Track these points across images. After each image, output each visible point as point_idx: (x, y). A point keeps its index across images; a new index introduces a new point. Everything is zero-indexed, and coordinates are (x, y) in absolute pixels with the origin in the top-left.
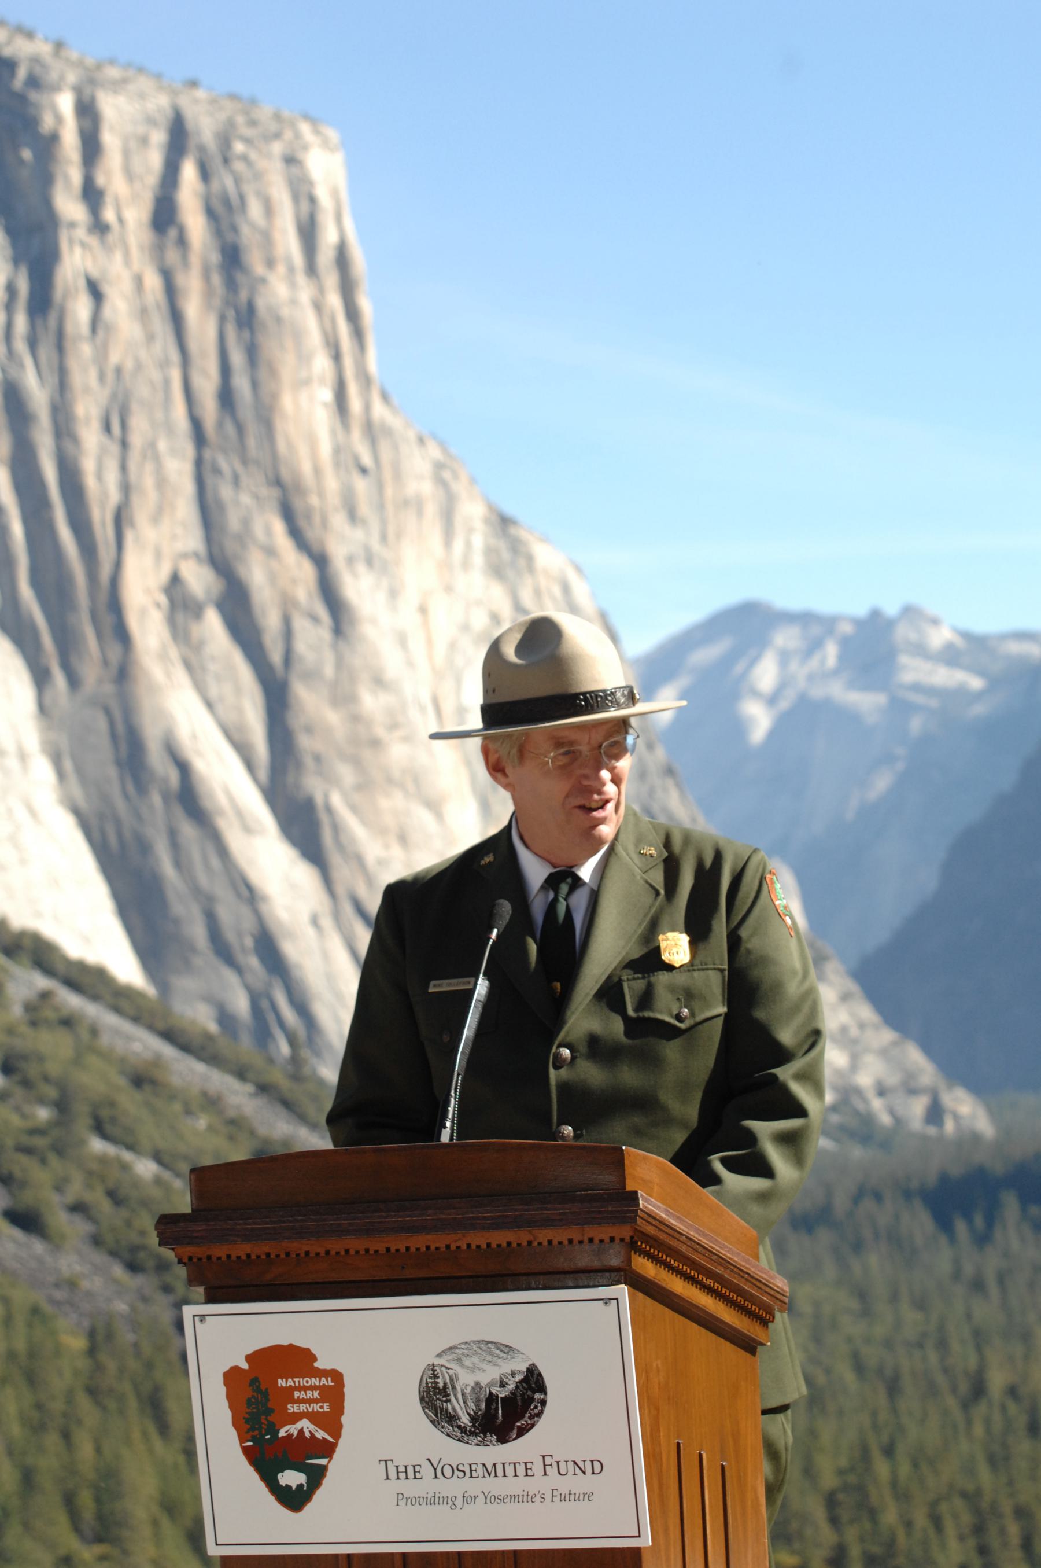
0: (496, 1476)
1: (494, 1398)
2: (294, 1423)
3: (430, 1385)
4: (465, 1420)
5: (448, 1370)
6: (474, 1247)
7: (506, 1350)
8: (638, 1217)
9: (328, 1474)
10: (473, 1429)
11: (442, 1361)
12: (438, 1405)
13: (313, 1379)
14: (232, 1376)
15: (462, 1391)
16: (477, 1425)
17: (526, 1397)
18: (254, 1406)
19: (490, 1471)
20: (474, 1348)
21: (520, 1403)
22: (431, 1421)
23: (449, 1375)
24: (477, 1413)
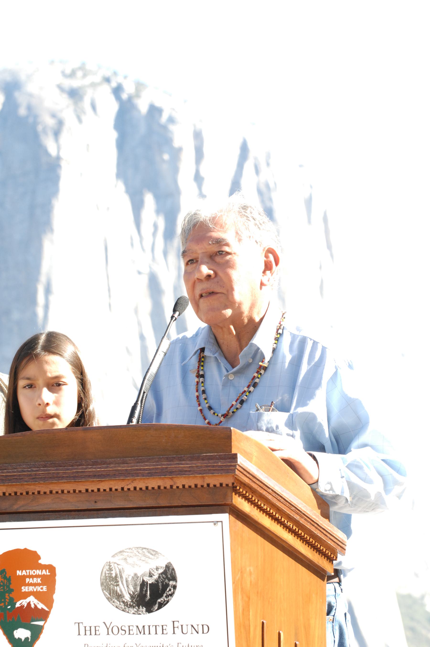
0: (144, 634)
2: (25, 599)
3: (107, 575)
4: (127, 598)
5: (118, 566)
7: (153, 553)
8: (236, 470)
9: (44, 631)
10: (132, 604)
11: (115, 560)
12: (111, 588)
13: (38, 571)
15: (126, 579)
17: (165, 583)
19: (141, 631)
21: (161, 587)
22: (107, 598)
23: (119, 569)
24: (135, 593)
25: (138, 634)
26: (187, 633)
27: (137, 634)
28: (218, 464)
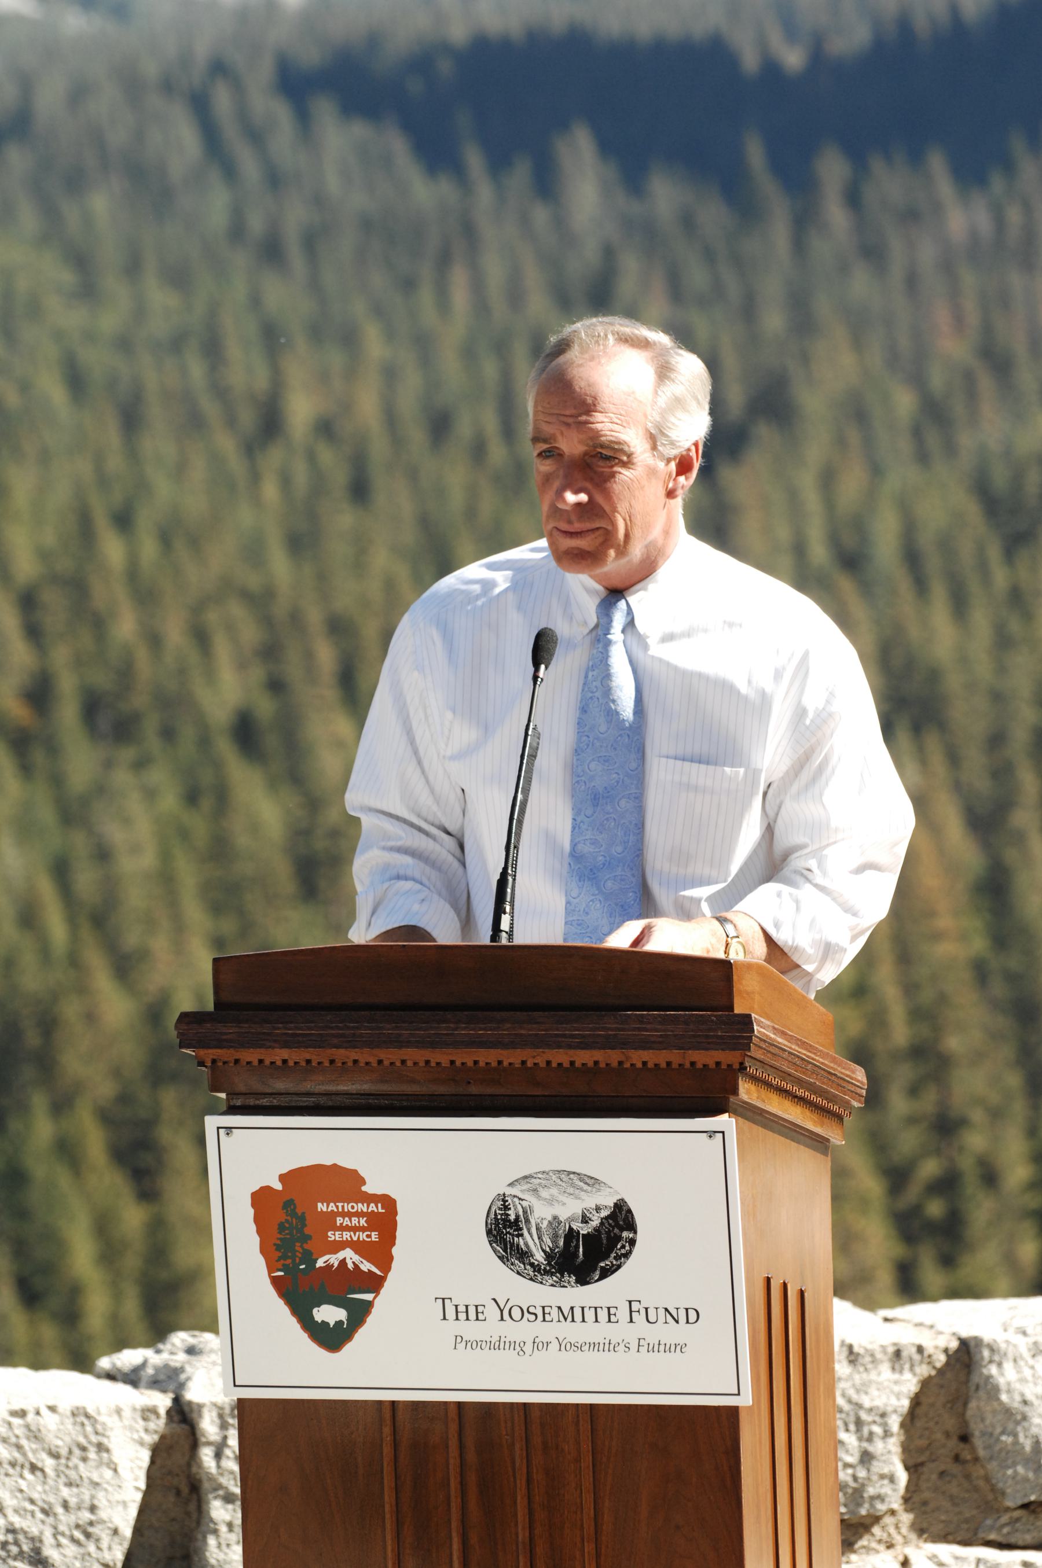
0: (573, 1320)
1: (575, 1234)
2: (335, 1252)
3: (499, 1217)
4: (539, 1257)
5: (521, 1202)
6: (554, 1065)
7: (590, 1182)
10: (548, 1268)
12: (508, 1239)
13: (360, 1205)
14: (261, 1198)
16: (553, 1263)
17: (612, 1235)
18: (287, 1232)
19: (566, 1316)
20: (553, 1178)
21: (605, 1242)
22: (499, 1257)
23: (522, 1207)
24: (554, 1250)
25: (560, 1320)
26: (657, 1321)
27: (559, 1321)
28: (716, 1034)
